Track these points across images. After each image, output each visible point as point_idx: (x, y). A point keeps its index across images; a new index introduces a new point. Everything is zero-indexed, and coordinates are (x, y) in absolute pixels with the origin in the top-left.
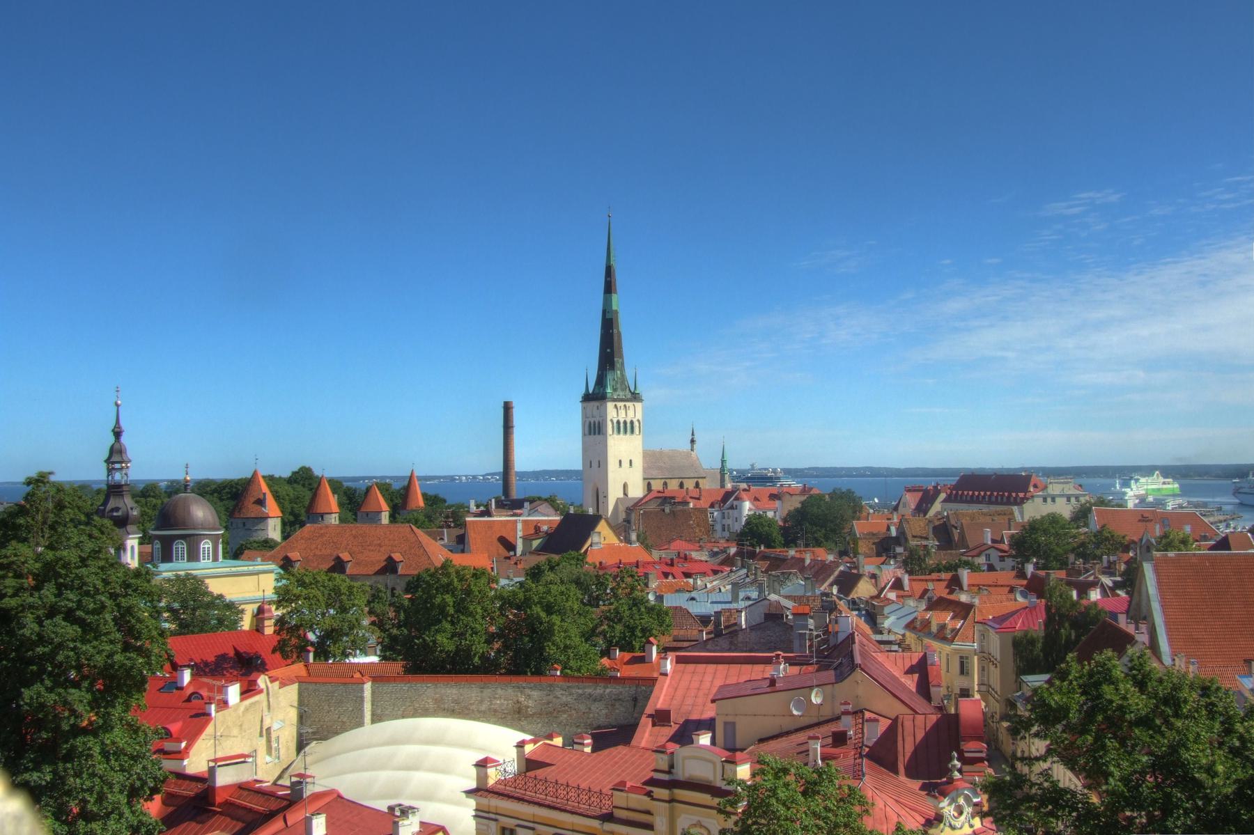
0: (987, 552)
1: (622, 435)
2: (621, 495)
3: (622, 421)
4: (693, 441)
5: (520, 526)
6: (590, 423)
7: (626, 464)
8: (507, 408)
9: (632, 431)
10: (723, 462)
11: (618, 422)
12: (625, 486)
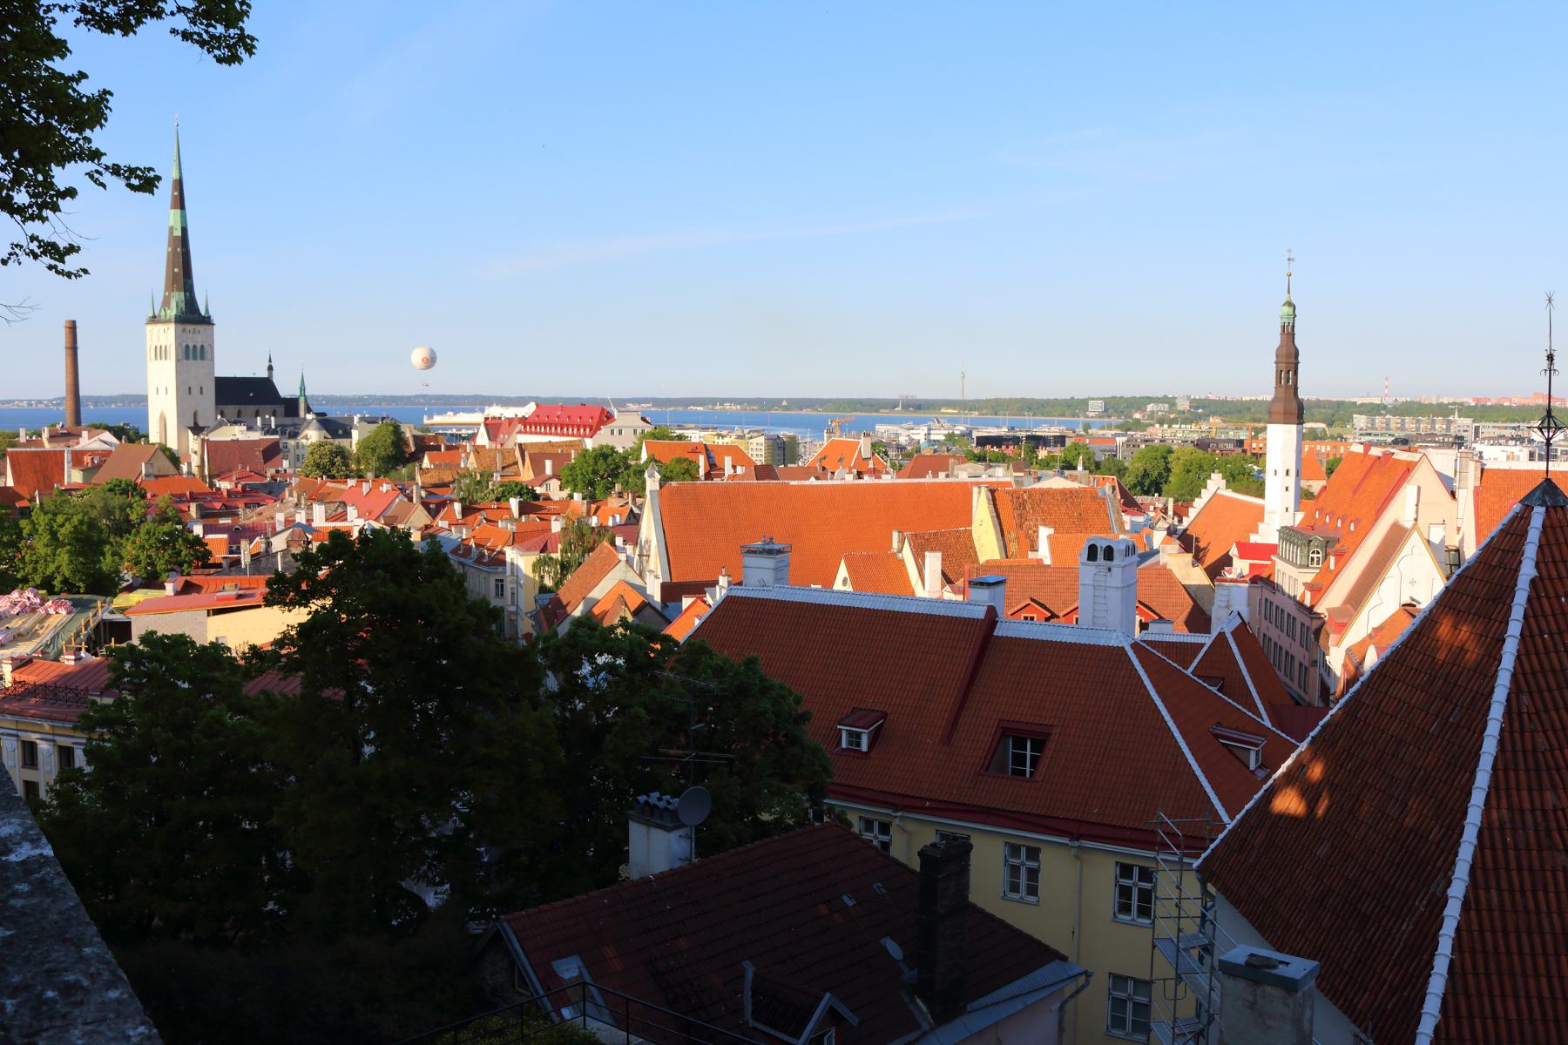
0: (548, 482)
1: (191, 361)
2: (192, 425)
3: (191, 346)
4: (270, 368)
5: (68, 458)
6: (156, 347)
7: (195, 391)
8: (72, 328)
9: (202, 358)
10: (303, 389)
11: (187, 346)
12: (195, 414)
